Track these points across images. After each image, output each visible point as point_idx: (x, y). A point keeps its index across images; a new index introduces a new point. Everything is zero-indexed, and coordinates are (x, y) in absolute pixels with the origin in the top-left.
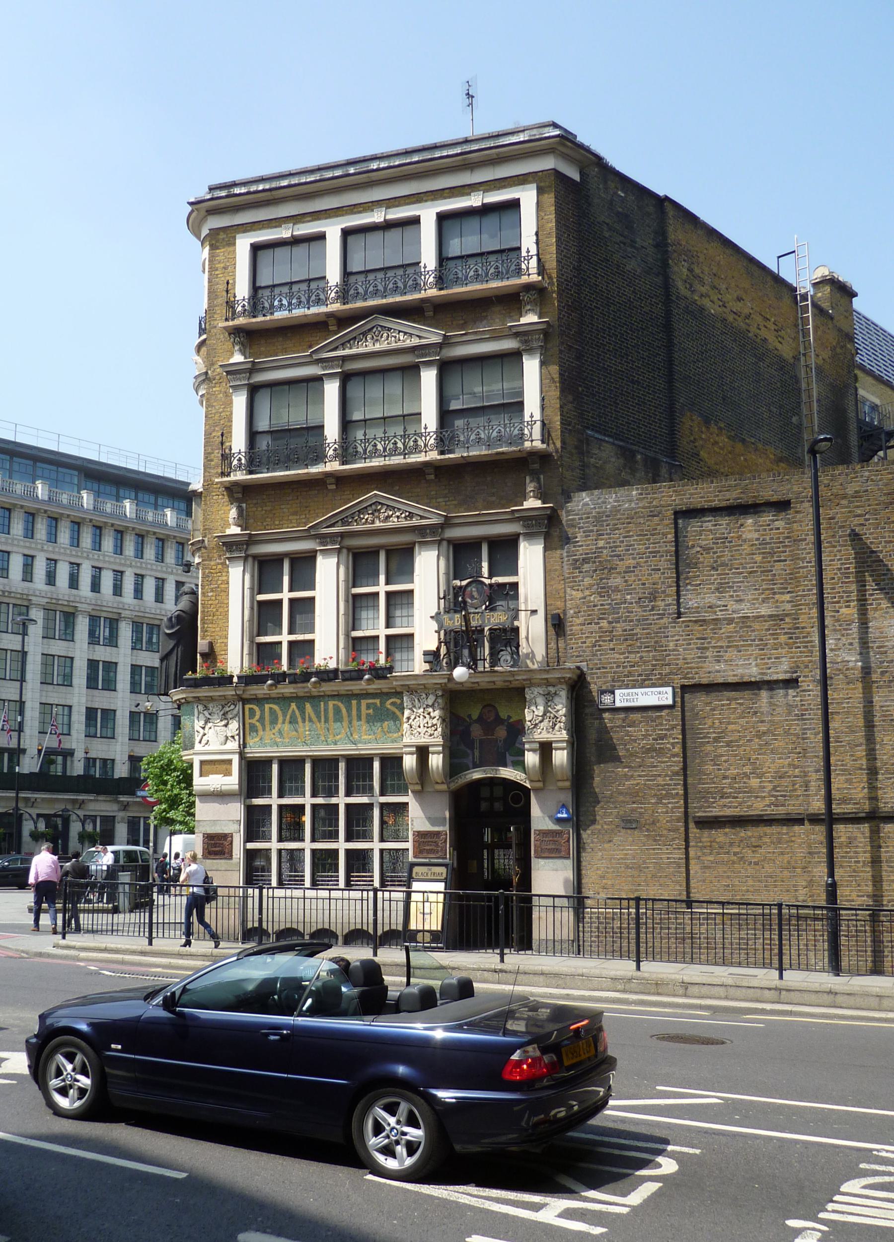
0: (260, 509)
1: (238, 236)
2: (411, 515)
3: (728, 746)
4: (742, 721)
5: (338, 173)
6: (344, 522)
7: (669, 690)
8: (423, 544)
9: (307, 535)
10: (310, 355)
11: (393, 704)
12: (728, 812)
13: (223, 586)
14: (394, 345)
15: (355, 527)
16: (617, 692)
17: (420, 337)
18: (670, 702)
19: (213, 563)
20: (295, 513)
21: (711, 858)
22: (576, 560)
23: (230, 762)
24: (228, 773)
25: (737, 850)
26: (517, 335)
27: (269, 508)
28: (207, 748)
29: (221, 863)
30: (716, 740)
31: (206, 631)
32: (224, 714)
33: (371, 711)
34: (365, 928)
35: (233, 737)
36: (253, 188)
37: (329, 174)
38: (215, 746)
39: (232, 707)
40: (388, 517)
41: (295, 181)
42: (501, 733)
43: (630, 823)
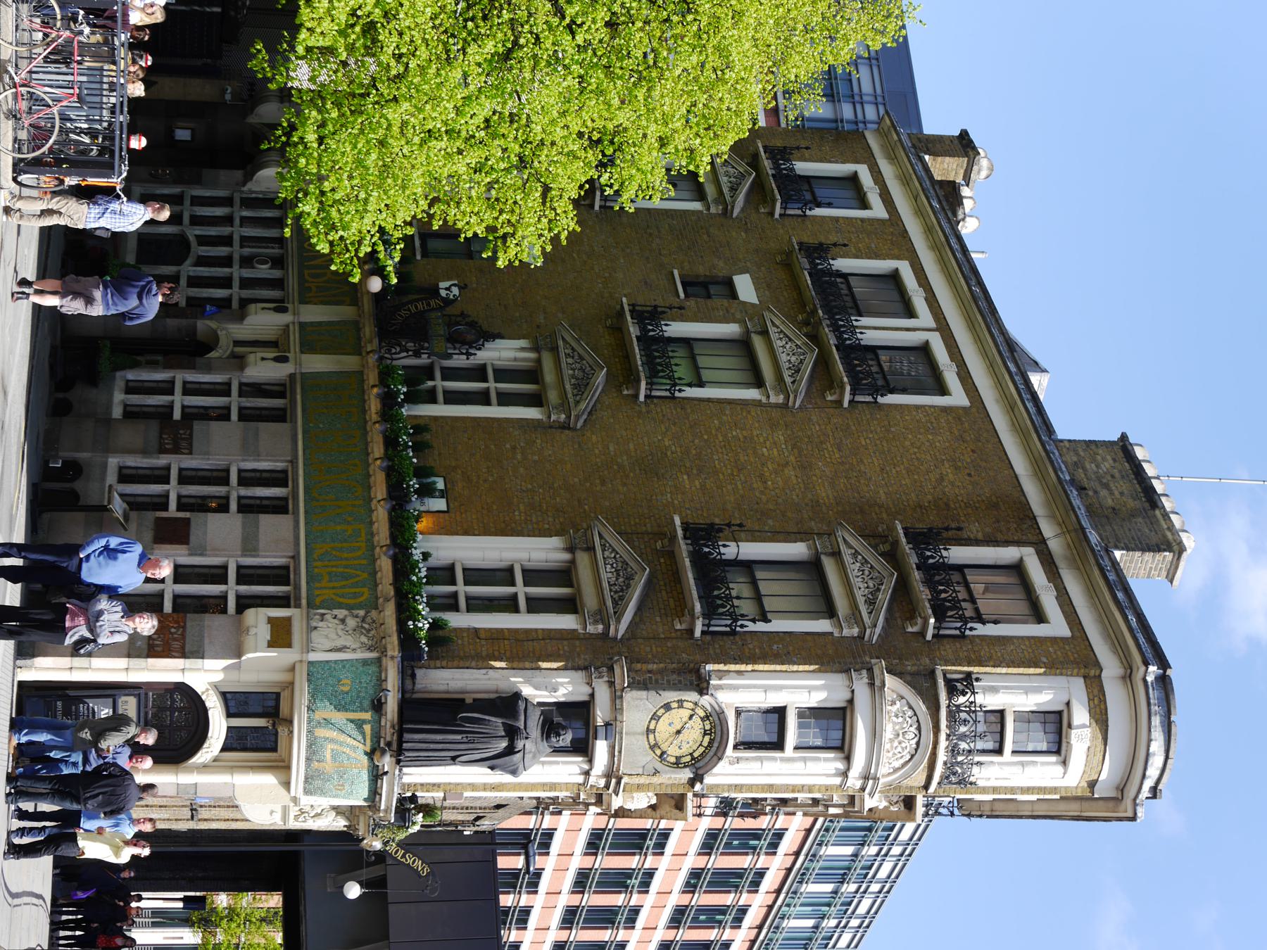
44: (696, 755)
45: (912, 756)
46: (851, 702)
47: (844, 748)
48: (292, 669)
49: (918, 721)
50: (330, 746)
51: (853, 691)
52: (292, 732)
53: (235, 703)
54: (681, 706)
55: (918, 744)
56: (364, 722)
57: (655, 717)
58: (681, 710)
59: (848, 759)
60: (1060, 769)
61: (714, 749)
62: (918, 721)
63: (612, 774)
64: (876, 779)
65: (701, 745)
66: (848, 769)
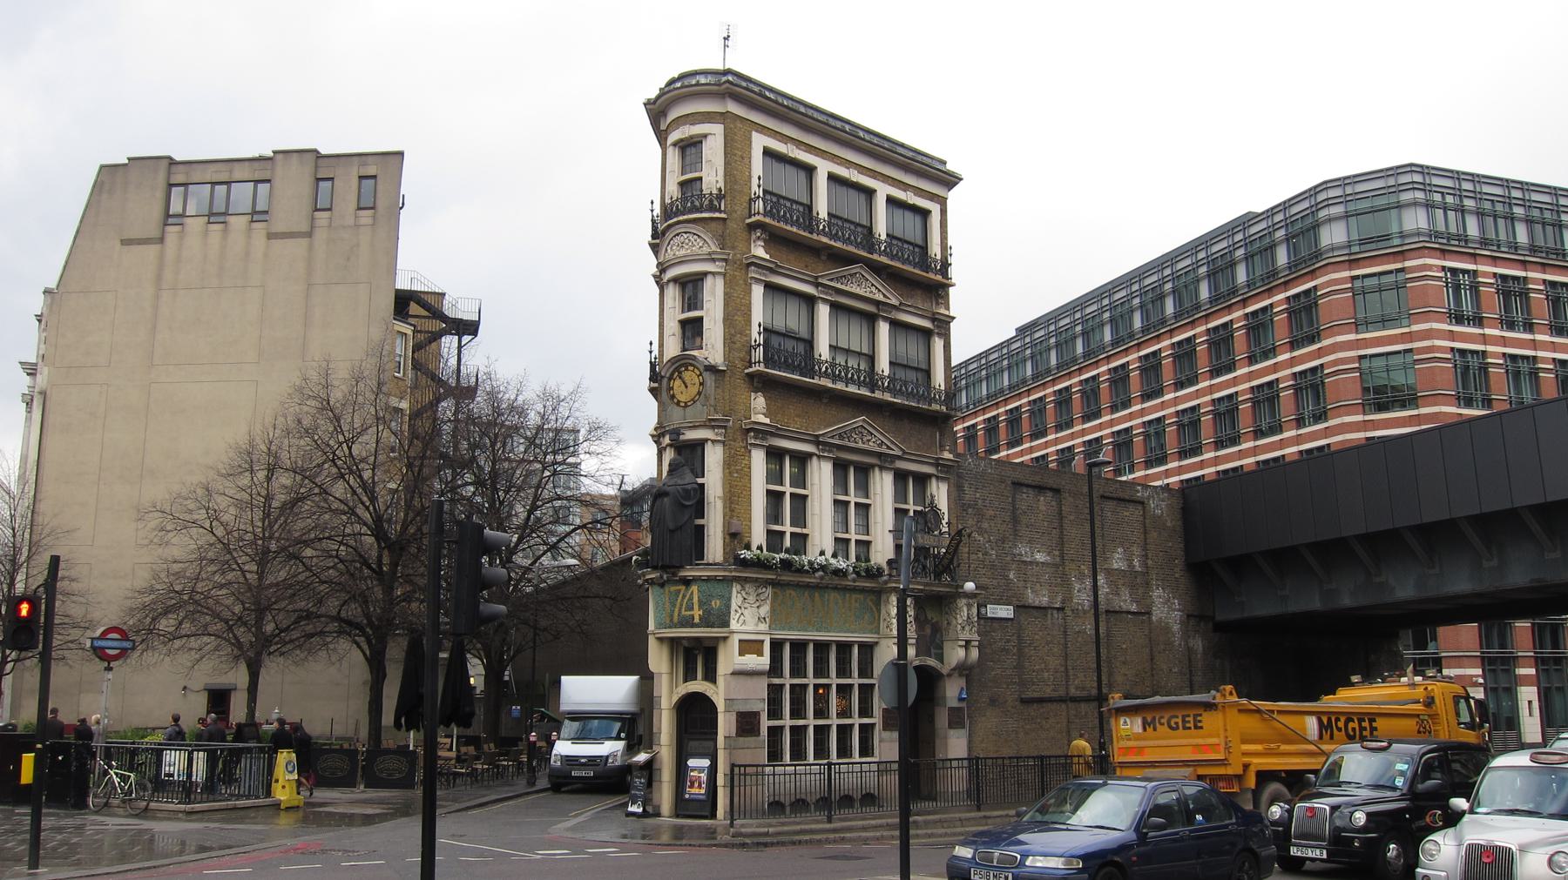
0: (773, 403)
1: (754, 134)
2: (880, 445)
3: (1035, 650)
4: (1040, 633)
5: (839, 124)
6: (841, 437)
7: (1012, 608)
8: (882, 468)
9: (816, 441)
10: (817, 278)
11: (871, 600)
12: (1036, 695)
13: (746, 469)
14: (868, 295)
15: (846, 443)
16: (988, 606)
17: (885, 296)
18: (1012, 616)
19: (737, 445)
20: (798, 416)
21: (1028, 727)
22: (965, 504)
23: (763, 641)
24: (760, 654)
25: (1039, 720)
26: (933, 320)
27: (779, 405)
28: (744, 628)
29: (750, 741)
30: (1030, 646)
31: (733, 511)
32: (757, 595)
33: (857, 605)
34: (872, 792)
35: (764, 618)
36: (780, 100)
37: (816, 115)
38: (750, 627)
39: (764, 590)
40: (869, 441)
41: (810, 112)
42: (928, 631)
43: (993, 702)
44: (698, 373)
45: (695, 234)
46: (675, 280)
47: (702, 276)
48: (661, 640)
49: (675, 236)
50: (683, 613)
51: (669, 281)
52: (684, 638)
53: (689, 675)
54: (672, 388)
55: (686, 233)
56: (669, 591)
57: (678, 403)
58: (675, 388)
59: (705, 274)
60: (709, 137)
61: (693, 362)
62: (675, 236)
63: (710, 424)
64: (710, 254)
65: (693, 371)
66: (710, 272)
